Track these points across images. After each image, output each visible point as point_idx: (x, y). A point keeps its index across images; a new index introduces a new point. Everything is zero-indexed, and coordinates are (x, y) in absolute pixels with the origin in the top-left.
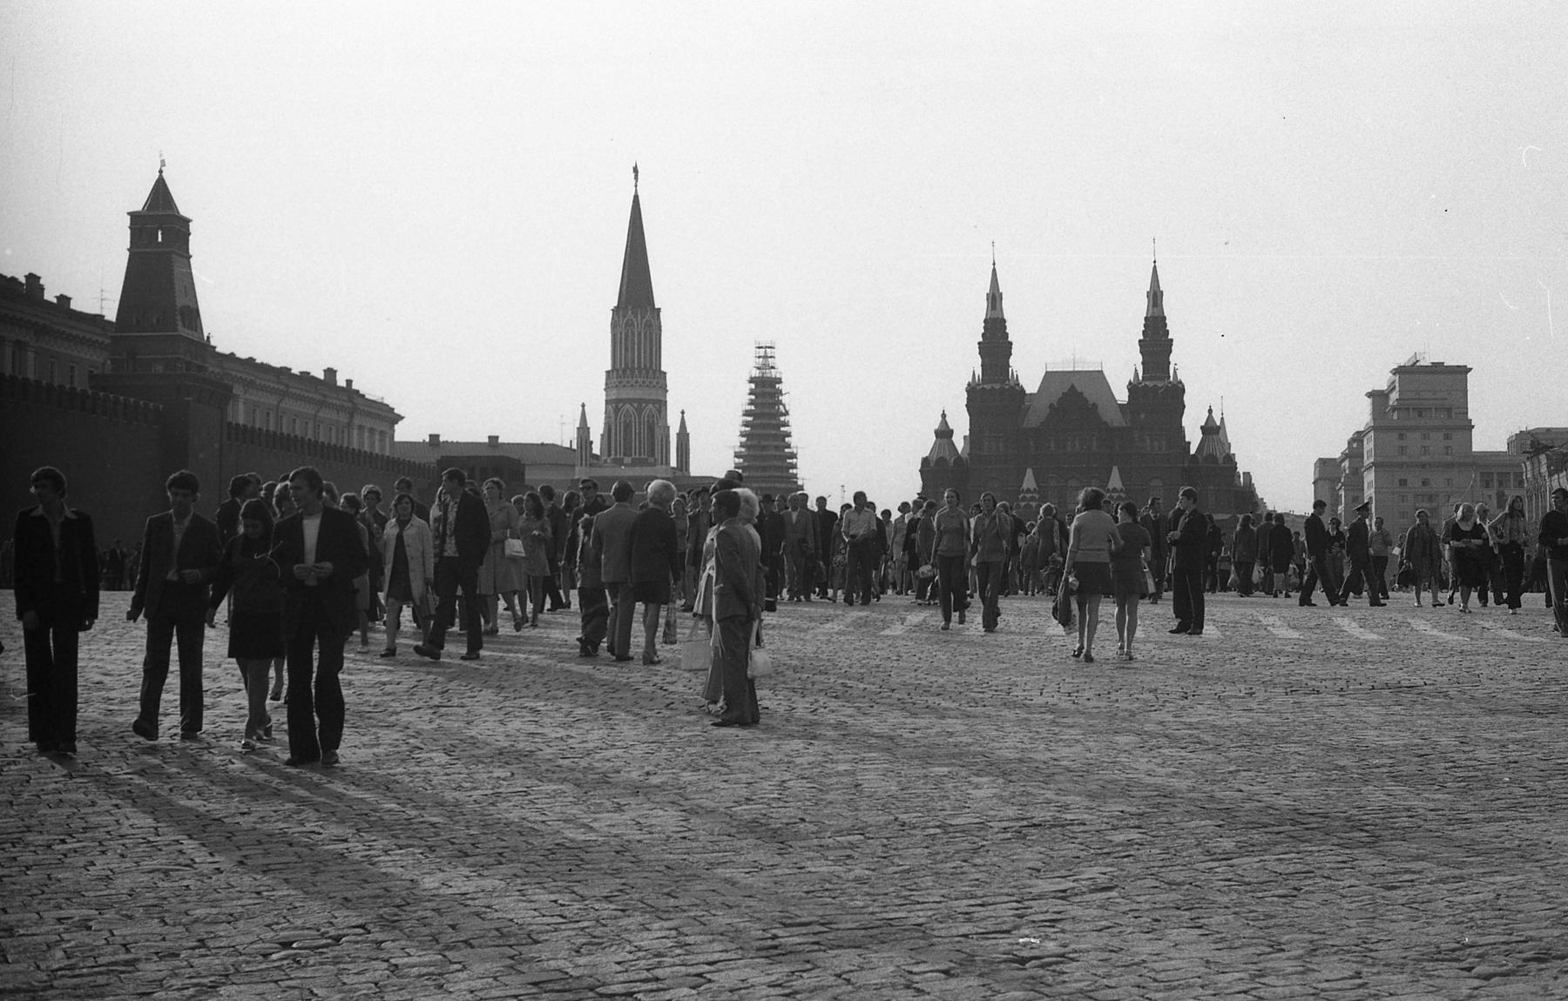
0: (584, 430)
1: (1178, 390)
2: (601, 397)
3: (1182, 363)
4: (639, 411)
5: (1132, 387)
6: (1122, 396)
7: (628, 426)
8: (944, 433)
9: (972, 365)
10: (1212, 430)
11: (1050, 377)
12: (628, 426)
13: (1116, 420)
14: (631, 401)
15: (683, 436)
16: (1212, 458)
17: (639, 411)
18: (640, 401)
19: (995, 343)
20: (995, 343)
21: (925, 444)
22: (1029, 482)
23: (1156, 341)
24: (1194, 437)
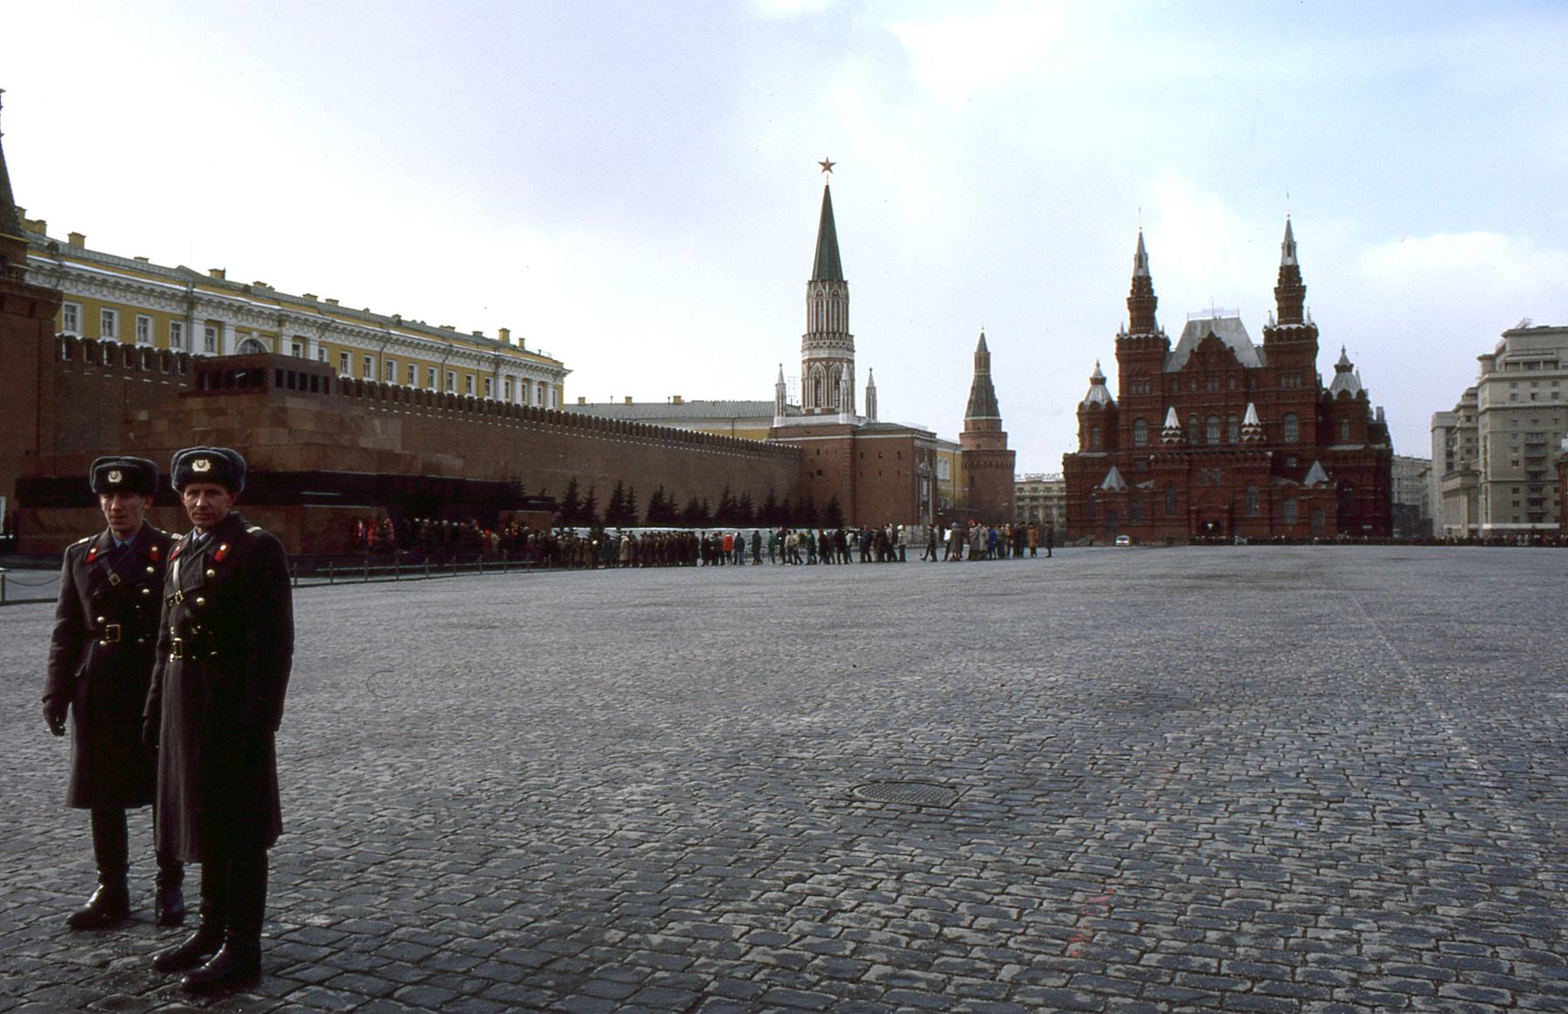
0: (781, 387)
1: (1311, 333)
3: (1314, 308)
4: (827, 368)
5: (1269, 333)
6: (1258, 339)
7: (818, 382)
8: (1099, 381)
9: (1122, 319)
10: (1344, 367)
11: (1191, 326)
12: (818, 382)
14: (820, 360)
15: (871, 393)
16: (1344, 394)
19: (1143, 300)
20: (1143, 300)
21: (1081, 391)
23: (1290, 288)
24: (1327, 375)
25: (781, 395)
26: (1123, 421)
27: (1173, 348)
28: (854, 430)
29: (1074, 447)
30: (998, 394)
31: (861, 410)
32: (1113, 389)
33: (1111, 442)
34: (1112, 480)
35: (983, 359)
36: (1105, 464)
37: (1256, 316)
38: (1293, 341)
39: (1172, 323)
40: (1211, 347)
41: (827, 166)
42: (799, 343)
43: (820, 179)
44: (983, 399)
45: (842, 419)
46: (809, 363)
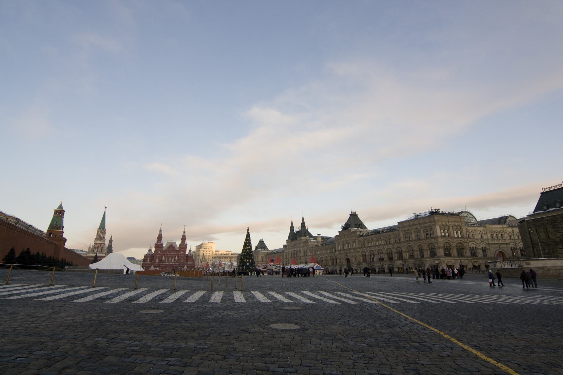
1: (187, 245)
6: (178, 246)
9: (156, 241)
19: (160, 238)
20: (160, 238)
22: (164, 258)
23: (184, 238)
24: (187, 252)
27: (164, 246)
34: (152, 267)
37: (178, 243)
38: (183, 246)
40: (171, 246)
41: (106, 207)
46: (96, 244)
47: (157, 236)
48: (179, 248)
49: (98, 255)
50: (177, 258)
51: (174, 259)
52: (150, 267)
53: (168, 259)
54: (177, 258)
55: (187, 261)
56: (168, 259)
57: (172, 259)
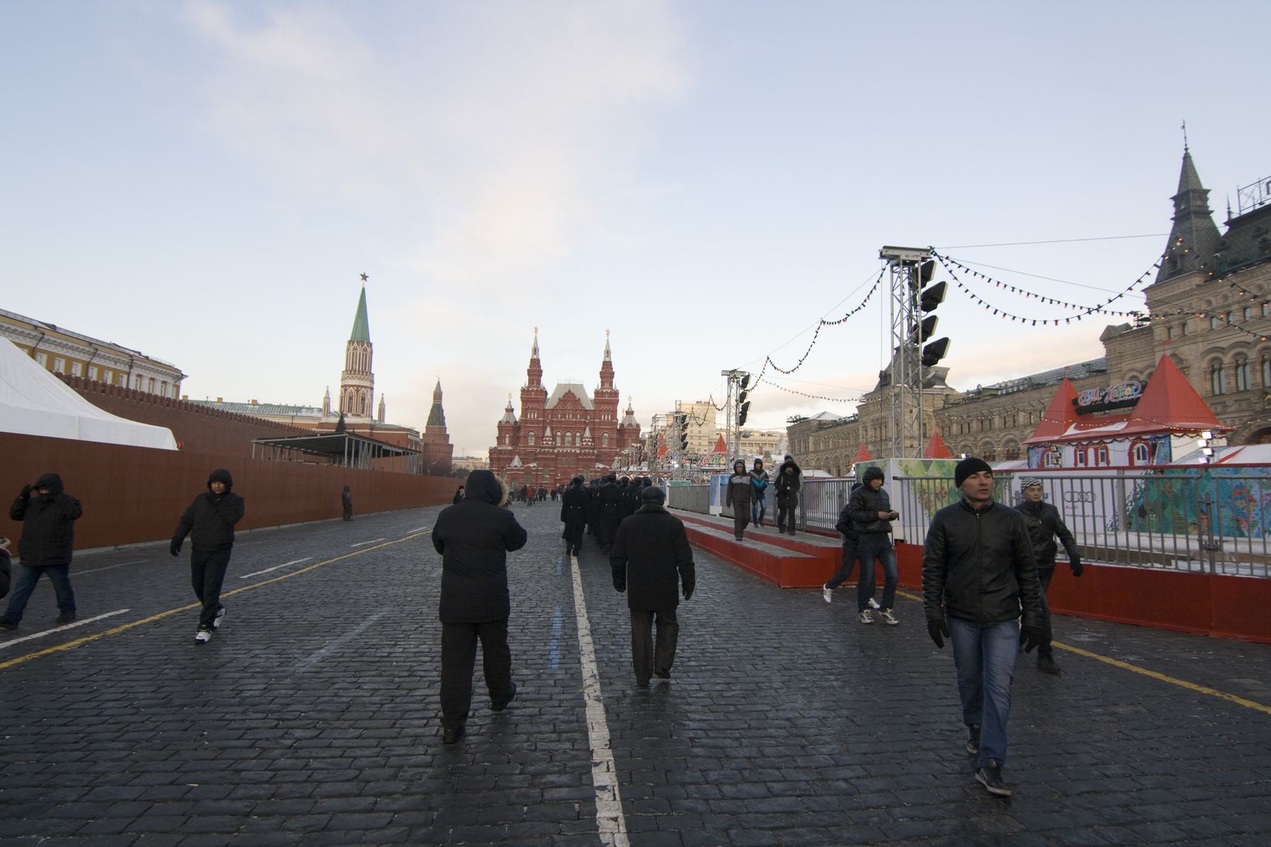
1: (616, 394)
2: (340, 384)
3: (618, 383)
4: (357, 391)
5: (597, 393)
6: (591, 396)
7: (351, 398)
8: (510, 410)
9: (524, 380)
10: (630, 413)
12: (351, 398)
13: (590, 407)
17: (357, 391)
18: (358, 386)
19: (535, 371)
20: (535, 371)
21: (501, 415)
22: (548, 432)
23: (607, 373)
24: (621, 416)
25: (327, 405)
26: (522, 434)
28: (372, 427)
29: (494, 444)
30: (445, 414)
31: (376, 417)
32: (518, 414)
33: (515, 441)
34: (517, 462)
35: (438, 396)
36: (511, 454)
37: (590, 385)
39: (550, 384)
40: (570, 397)
41: (364, 277)
42: (340, 375)
43: (361, 283)
44: (437, 415)
45: (366, 420)
47: (527, 365)
48: (596, 402)
49: (347, 420)
50: (587, 433)
51: (582, 437)
52: (511, 460)
53: (563, 437)
54: (587, 433)
55: (621, 443)
56: (563, 437)
57: (574, 437)
